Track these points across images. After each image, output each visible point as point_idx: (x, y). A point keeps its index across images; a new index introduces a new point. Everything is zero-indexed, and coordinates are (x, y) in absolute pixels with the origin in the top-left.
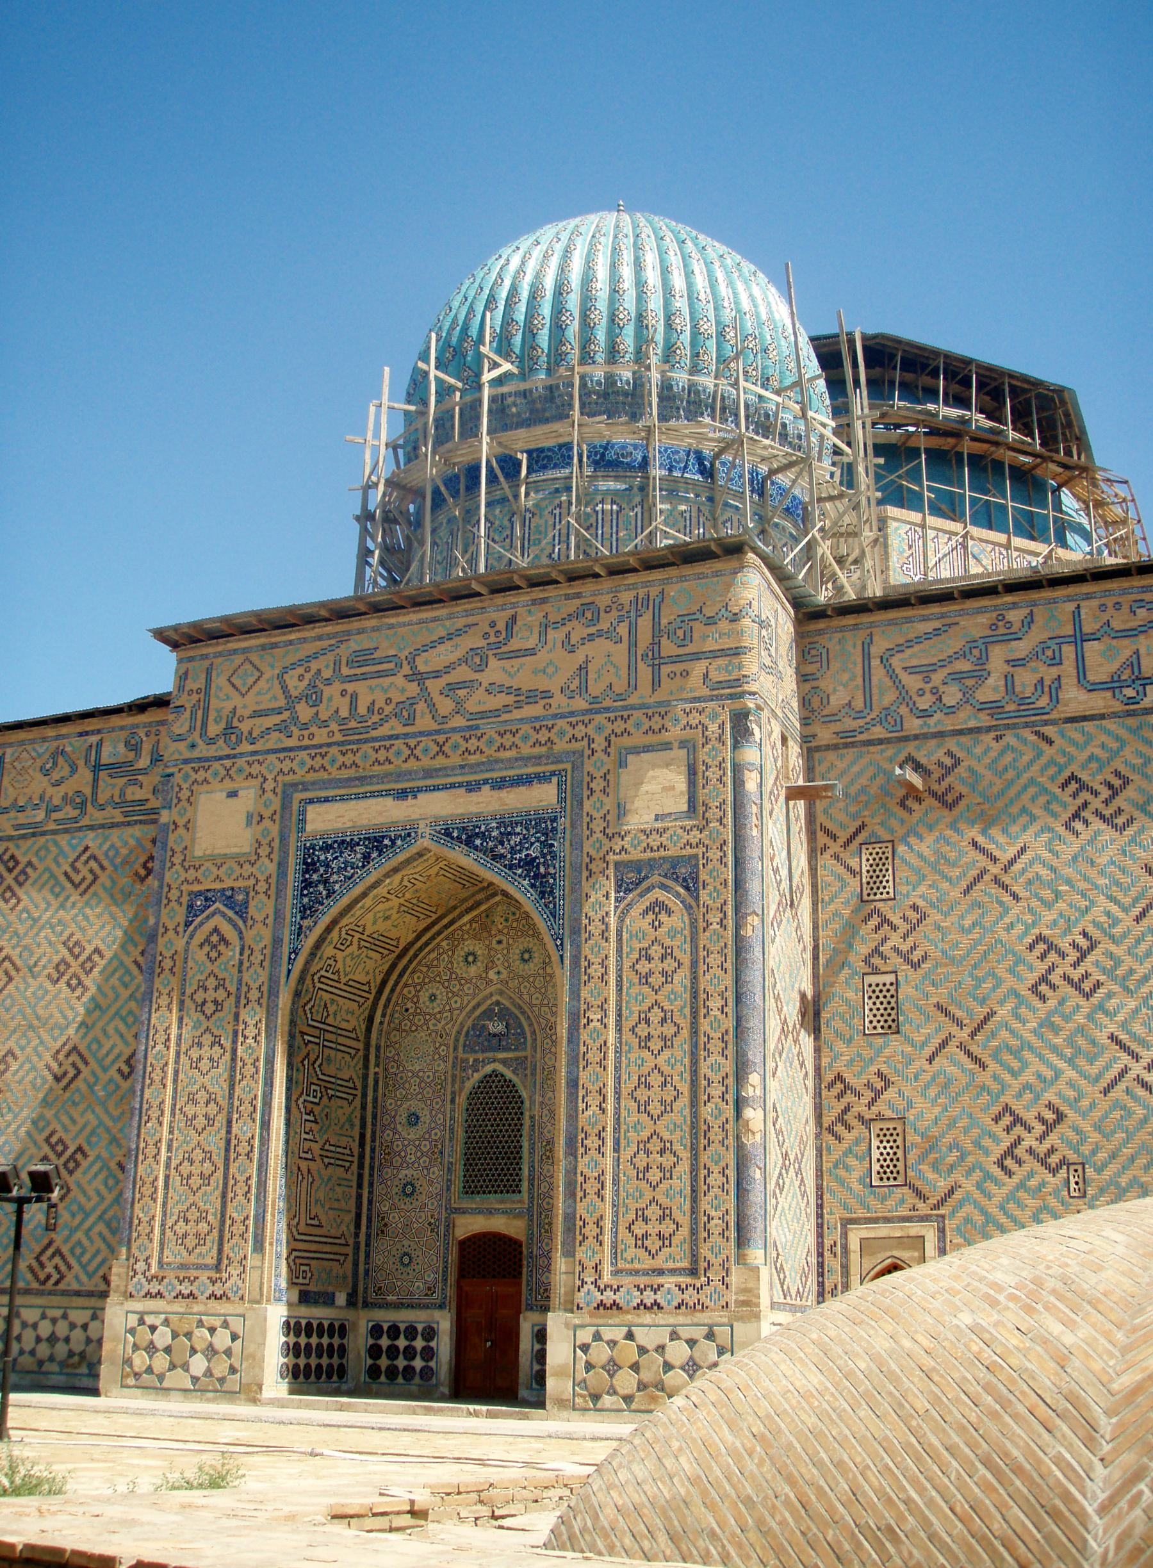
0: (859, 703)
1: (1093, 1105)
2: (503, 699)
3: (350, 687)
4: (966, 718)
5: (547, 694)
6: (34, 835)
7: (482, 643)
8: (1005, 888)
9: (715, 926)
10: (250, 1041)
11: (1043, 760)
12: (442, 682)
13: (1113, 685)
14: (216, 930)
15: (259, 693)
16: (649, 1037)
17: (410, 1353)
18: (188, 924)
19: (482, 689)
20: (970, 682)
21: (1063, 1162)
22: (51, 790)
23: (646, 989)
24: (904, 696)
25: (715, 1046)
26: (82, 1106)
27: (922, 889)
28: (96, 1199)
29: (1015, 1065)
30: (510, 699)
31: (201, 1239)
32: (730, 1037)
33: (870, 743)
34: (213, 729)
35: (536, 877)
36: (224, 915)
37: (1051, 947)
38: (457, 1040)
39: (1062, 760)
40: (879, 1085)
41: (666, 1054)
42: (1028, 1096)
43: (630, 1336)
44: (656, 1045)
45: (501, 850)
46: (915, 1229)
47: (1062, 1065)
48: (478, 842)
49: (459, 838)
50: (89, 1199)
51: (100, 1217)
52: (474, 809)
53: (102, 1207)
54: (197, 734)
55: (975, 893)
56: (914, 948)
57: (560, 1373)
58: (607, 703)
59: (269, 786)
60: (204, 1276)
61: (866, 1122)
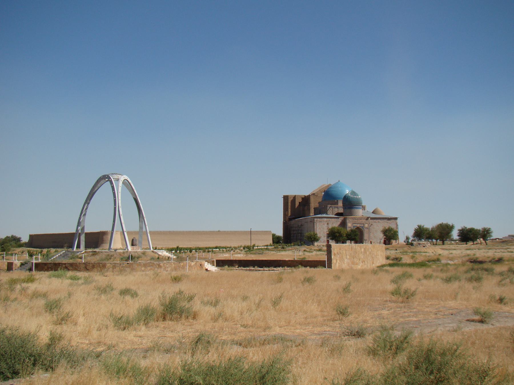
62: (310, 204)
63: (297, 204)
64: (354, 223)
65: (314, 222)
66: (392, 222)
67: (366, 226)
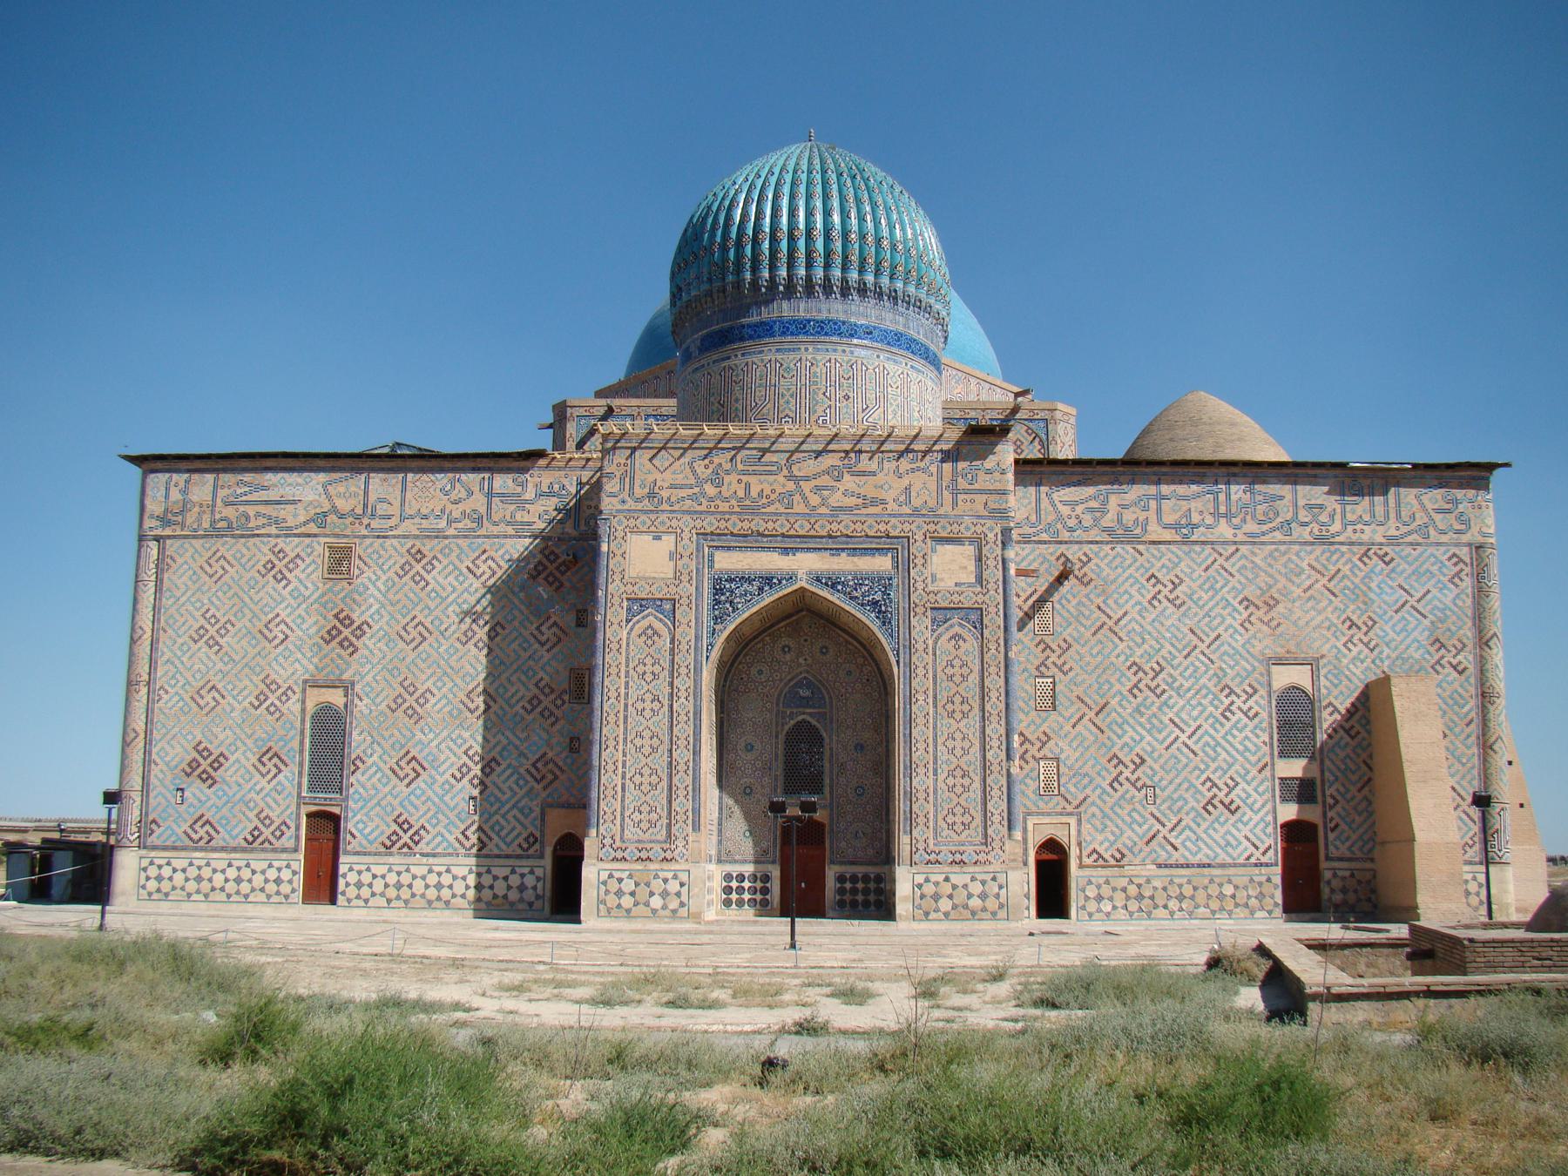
0: (1033, 518)
1: (1160, 756)
2: (852, 501)
3: (745, 478)
4: (1094, 534)
5: (883, 502)
6: (437, 537)
7: (840, 463)
8: (1116, 634)
9: (993, 651)
10: (683, 700)
11: (1138, 564)
12: (813, 483)
13: (1176, 527)
14: (650, 626)
15: (674, 473)
16: (954, 711)
17: (854, 891)
18: (628, 621)
19: (840, 492)
20: (1098, 514)
21: (1144, 785)
22: (450, 507)
23: (951, 684)
24: (1060, 518)
25: (994, 719)
26: (494, 730)
27: (1069, 630)
28: (509, 794)
29: (1120, 732)
31: (652, 824)
32: (1003, 715)
33: (1040, 542)
34: (638, 492)
35: (880, 612)
36: (656, 618)
37: (1140, 668)
38: (778, 699)
39: (1147, 565)
40: (1045, 739)
41: (965, 721)
42: (1126, 749)
43: (947, 879)
44: (958, 716)
45: (855, 594)
46: (1064, 819)
47: (1144, 733)
48: (840, 587)
49: (826, 584)
50: (504, 793)
51: (514, 806)
52: (836, 567)
53: (515, 799)
54: (625, 495)
55: (1099, 636)
56: (1064, 663)
57: (905, 899)
58: (924, 512)
59: (686, 535)
60: (657, 847)
61: (1037, 760)
64: (736, 525)
66: (1392, 541)
67: (947, 583)
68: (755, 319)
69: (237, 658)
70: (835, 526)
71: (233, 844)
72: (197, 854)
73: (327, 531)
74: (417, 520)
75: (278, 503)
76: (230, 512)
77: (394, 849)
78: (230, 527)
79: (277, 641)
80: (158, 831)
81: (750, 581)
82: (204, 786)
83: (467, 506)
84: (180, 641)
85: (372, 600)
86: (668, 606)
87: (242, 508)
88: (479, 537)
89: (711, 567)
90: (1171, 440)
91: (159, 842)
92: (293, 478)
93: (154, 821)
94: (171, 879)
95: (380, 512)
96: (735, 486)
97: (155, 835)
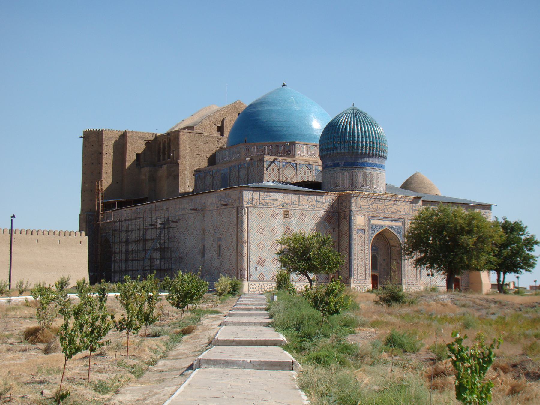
2: (395, 211)
22: (308, 203)
30: (396, 211)
52: (392, 224)
54: (356, 207)
60: (364, 281)
62: (178, 157)
63: (130, 158)
64: (375, 214)
65: (242, 207)
68: (360, 161)
69: (267, 237)
70: (392, 216)
71: (268, 280)
72: (261, 282)
73: (284, 208)
74: (302, 206)
75: (273, 200)
76: (263, 202)
77: (301, 281)
78: (263, 205)
79: (275, 233)
80: (252, 277)
81: (377, 226)
82: (261, 267)
83: (312, 203)
84: (254, 232)
85: (294, 224)
86: (364, 231)
87: (266, 201)
88: (314, 211)
89: (371, 223)
90: (419, 187)
91: (253, 280)
92: (276, 194)
93: (251, 275)
94: (256, 288)
95: (294, 204)
96: (375, 206)
97: (252, 278)
